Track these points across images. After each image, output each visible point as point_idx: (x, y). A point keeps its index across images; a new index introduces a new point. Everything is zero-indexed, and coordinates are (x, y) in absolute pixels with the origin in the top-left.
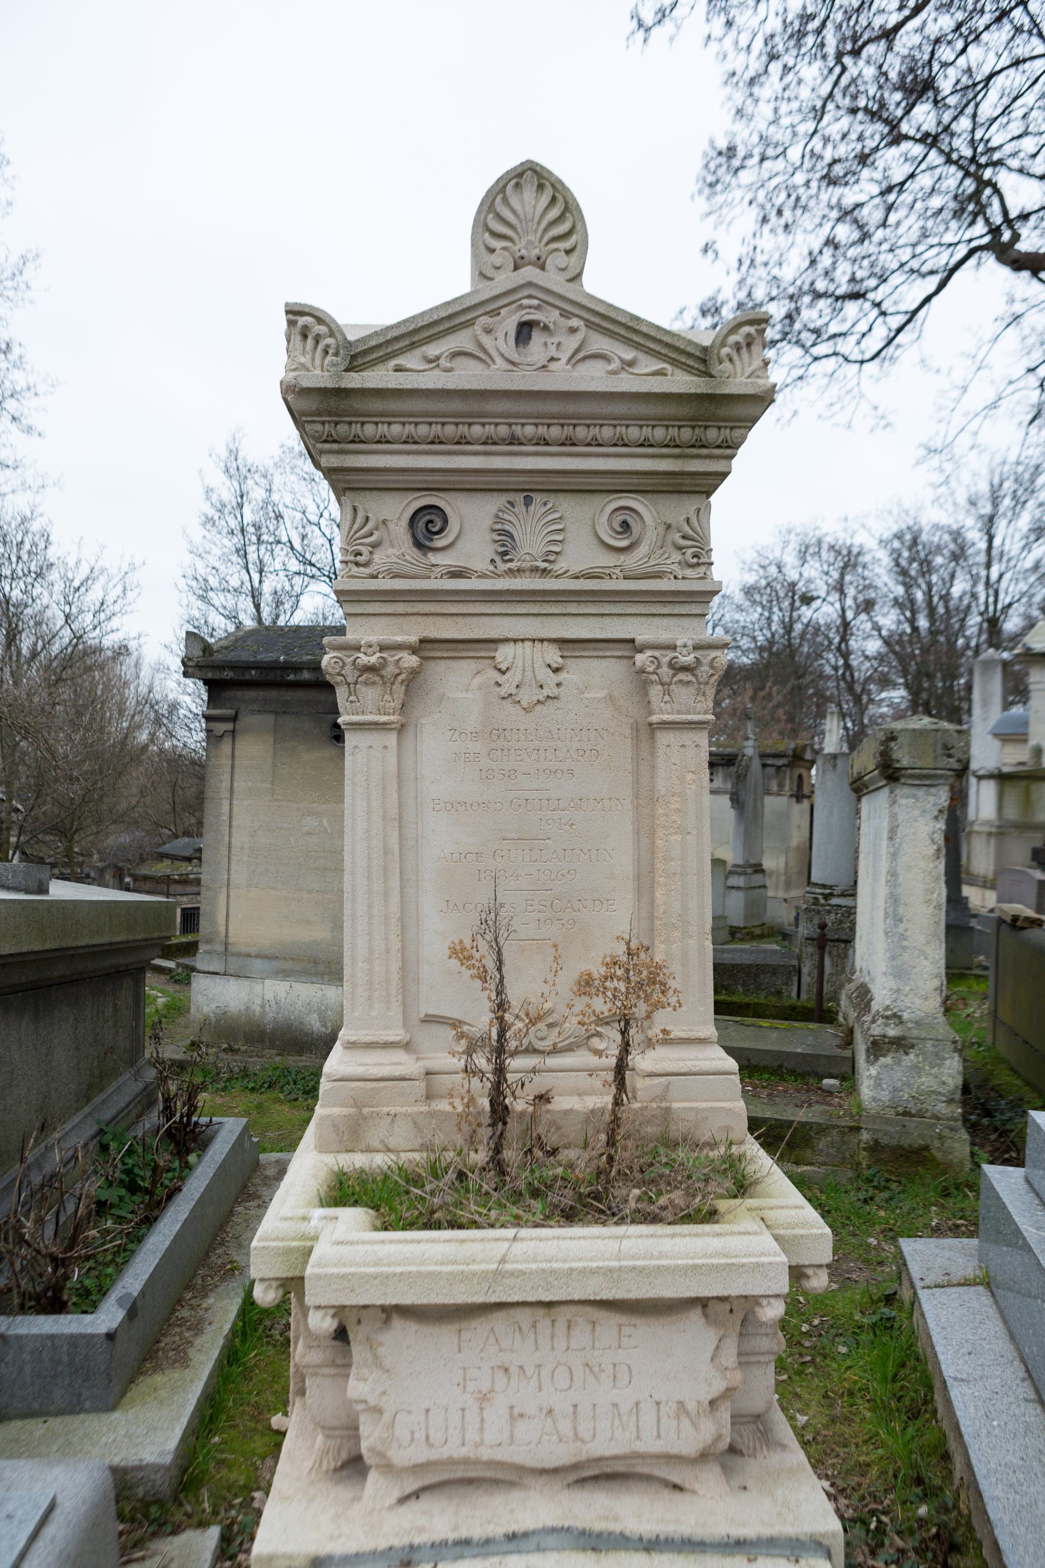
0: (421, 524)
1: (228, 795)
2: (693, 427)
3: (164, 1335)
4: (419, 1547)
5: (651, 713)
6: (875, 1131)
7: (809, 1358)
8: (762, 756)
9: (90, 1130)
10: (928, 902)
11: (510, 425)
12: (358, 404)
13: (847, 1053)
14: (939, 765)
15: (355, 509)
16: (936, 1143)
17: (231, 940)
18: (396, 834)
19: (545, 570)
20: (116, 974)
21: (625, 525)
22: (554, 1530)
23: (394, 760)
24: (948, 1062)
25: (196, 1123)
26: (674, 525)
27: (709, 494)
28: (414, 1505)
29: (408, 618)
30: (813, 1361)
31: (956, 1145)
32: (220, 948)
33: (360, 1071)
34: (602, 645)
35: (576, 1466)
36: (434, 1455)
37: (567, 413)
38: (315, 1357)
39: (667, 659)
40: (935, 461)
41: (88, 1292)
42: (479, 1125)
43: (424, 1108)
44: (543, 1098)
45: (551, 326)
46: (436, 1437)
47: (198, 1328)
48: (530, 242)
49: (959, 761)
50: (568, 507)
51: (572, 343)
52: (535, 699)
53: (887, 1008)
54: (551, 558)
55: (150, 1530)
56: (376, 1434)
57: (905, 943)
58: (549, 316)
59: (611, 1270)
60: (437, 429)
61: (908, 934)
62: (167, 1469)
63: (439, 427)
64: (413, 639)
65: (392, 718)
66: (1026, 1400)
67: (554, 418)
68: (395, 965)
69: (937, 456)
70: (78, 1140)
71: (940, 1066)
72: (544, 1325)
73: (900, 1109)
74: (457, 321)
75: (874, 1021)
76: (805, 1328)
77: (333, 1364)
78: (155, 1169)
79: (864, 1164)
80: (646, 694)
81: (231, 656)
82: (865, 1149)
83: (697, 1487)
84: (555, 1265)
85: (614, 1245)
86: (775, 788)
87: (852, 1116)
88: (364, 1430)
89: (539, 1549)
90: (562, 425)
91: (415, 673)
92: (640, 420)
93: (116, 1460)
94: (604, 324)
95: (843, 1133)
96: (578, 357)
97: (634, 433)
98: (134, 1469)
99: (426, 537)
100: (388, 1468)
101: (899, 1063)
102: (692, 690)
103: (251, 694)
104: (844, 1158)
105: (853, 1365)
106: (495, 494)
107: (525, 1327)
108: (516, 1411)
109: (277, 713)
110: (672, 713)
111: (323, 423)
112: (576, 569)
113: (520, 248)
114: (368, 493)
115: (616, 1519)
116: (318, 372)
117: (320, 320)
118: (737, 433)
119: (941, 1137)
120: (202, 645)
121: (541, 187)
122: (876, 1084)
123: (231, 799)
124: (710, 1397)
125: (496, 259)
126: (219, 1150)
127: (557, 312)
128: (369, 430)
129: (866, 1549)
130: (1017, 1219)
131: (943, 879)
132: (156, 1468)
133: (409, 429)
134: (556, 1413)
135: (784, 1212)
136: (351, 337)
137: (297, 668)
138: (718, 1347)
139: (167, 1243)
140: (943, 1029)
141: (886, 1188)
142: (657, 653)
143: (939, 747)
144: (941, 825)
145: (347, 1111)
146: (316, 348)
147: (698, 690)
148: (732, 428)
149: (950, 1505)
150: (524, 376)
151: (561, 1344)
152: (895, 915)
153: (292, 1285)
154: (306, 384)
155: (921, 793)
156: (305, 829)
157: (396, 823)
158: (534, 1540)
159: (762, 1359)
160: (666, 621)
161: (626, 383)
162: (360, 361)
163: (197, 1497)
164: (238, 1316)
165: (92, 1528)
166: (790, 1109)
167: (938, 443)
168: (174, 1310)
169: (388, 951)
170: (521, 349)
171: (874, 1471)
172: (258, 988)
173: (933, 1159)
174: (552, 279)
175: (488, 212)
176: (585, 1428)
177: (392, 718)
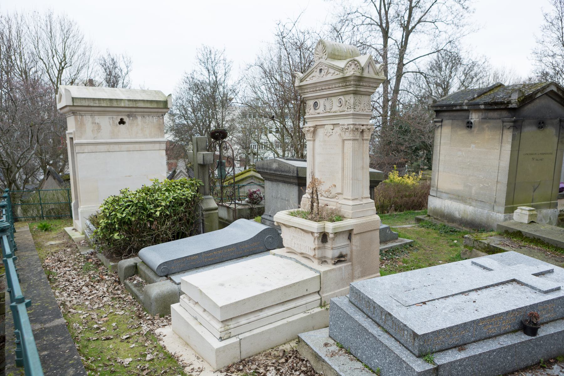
32: (436, 189)
50: (333, 99)
97: (337, 85)
103: (446, 114)
109: (452, 119)
128: (306, 91)
172: (444, 202)
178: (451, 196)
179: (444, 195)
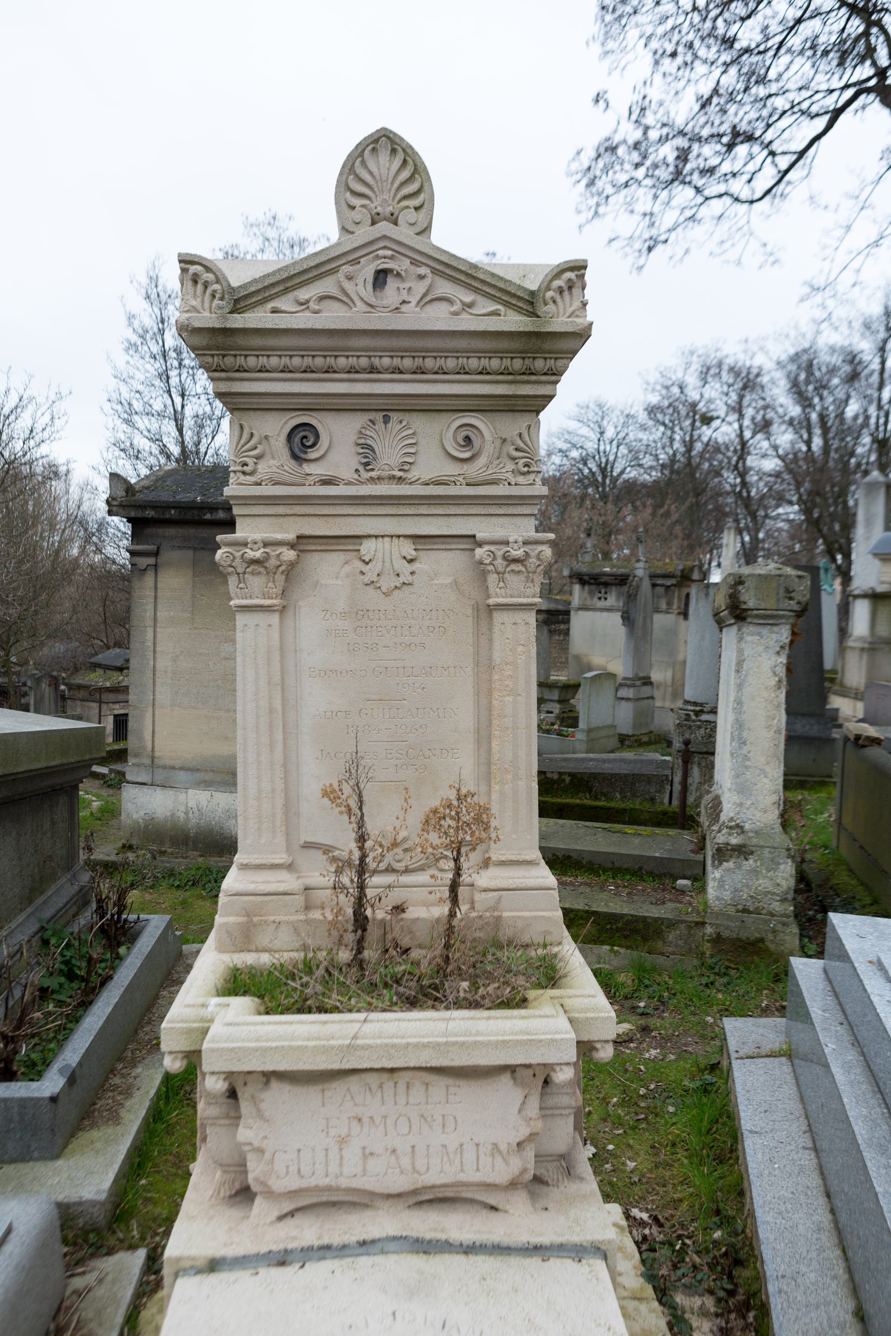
0: (297, 439)
1: (152, 624)
2: (524, 358)
3: (100, 1099)
4: (292, 1251)
5: (488, 597)
6: (718, 925)
7: (643, 1116)
8: (652, 576)
9: (33, 927)
10: (769, 727)
11: (370, 357)
12: (241, 341)
13: (700, 857)
14: (781, 606)
15: (241, 427)
16: (770, 936)
17: (157, 754)
18: (279, 696)
19: (400, 478)
20: (54, 792)
21: (468, 439)
22: (394, 1238)
23: (276, 636)
24: (782, 867)
25: (126, 920)
26: (509, 439)
27: (538, 412)
28: (289, 1222)
29: (287, 518)
30: (646, 1119)
31: (787, 938)
32: (147, 761)
33: (251, 887)
34: (449, 540)
35: (415, 1192)
36: (304, 1184)
37: (417, 349)
38: (213, 1111)
39: (502, 552)
40: (819, 298)
41: (34, 1064)
42: (346, 931)
43: (302, 917)
44: (399, 909)
45: (403, 273)
46: (306, 1170)
47: (128, 1092)
48: (385, 200)
49: (799, 603)
50: (420, 424)
51: (420, 288)
52: (393, 585)
53: (732, 819)
54: (406, 467)
55: (90, 1251)
56: (260, 1168)
57: (748, 763)
58: (401, 265)
59: (438, 1044)
60: (308, 361)
61: (750, 755)
62: (102, 1204)
63: (310, 359)
64: (291, 536)
65: (275, 602)
66: (804, 1148)
67: (406, 351)
68: (280, 802)
69: (821, 294)
70: (22, 937)
71: (775, 870)
72: (389, 1085)
73: (740, 907)
74: (323, 269)
75: (719, 831)
76: (642, 1091)
77: (227, 1117)
78: (90, 959)
79: (708, 953)
80: (485, 580)
81: (151, 497)
82: (708, 941)
83: (508, 1207)
84: (395, 1041)
85: (442, 1025)
86: (664, 606)
87: (698, 913)
88: (250, 1165)
89: (383, 1252)
90: (414, 357)
91: (292, 565)
92: (479, 353)
93: (60, 1198)
94: (448, 271)
95: (690, 927)
96: (426, 300)
97: (473, 363)
98: (75, 1204)
99: (301, 450)
100: (270, 1194)
101: (739, 867)
102: (522, 577)
103: (172, 531)
104: (690, 949)
105: (676, 1119)
106: (359, 413)
107: (374, 1087)
108: (368, 1151)
109: (195, 549)
110: (506, 597)
111: (213, 356)
112: (426, 477)
113: (376, 205)
114: (252, 413)
115: (443, 1230)
116: (207, 314)
117: (208, 269)
118: (560, 363)
119: (774, 931)
120: (125, 486)
121: (394, 151)
122: (722, 885)
123: (155, 627)
124: (518, 1140)
125: (356, 215)
126: (146, 943)
127: (408, 261)
128: (252, 361)
129: (670, 1264)
130: (808, 1003)
131: (784, 706)
132: (93, 1203)
133: (285, 361)
134: (398, 1152)
135: (579, 1000)
136: (235, 283)
137: (213, 508)
138: (524, 1103)
139: (101, 1023)
140: (779, 838)
141: (725, 974)
142: (492, 548)
143: (782, 591)
144: (783, 659)
145: (241, 919)
146: (205, 292)
147: (528, 577)
148: (556, 359)
149: (740, 1231)
150: (380, 317)
151: (402, 1100)
152: (740, 738)
153: (193, 1058)
154: (197, 324)
155: (765, 631)
156: (223, 655)
157: (279, 688)
158: (380, 1245)
159: (563, 1112)
160: (501, 520)
161: (466, 323)
162: (242, 304)
163: (127, 1226)
164: (162, 1082)
165: (41, 1249)
166: (646, 906)
167: (821, 282)
168: (107, 1079)
169: (273, 791)
170: (378, 293)
171: (685, 1205)
172: (182, 797)
173: (767, 950)
174: (404, 233)
175: (349, 174)
176: (421, 1164)
177: (275, 602)
178: (209, 777)
179: (182, 775)
